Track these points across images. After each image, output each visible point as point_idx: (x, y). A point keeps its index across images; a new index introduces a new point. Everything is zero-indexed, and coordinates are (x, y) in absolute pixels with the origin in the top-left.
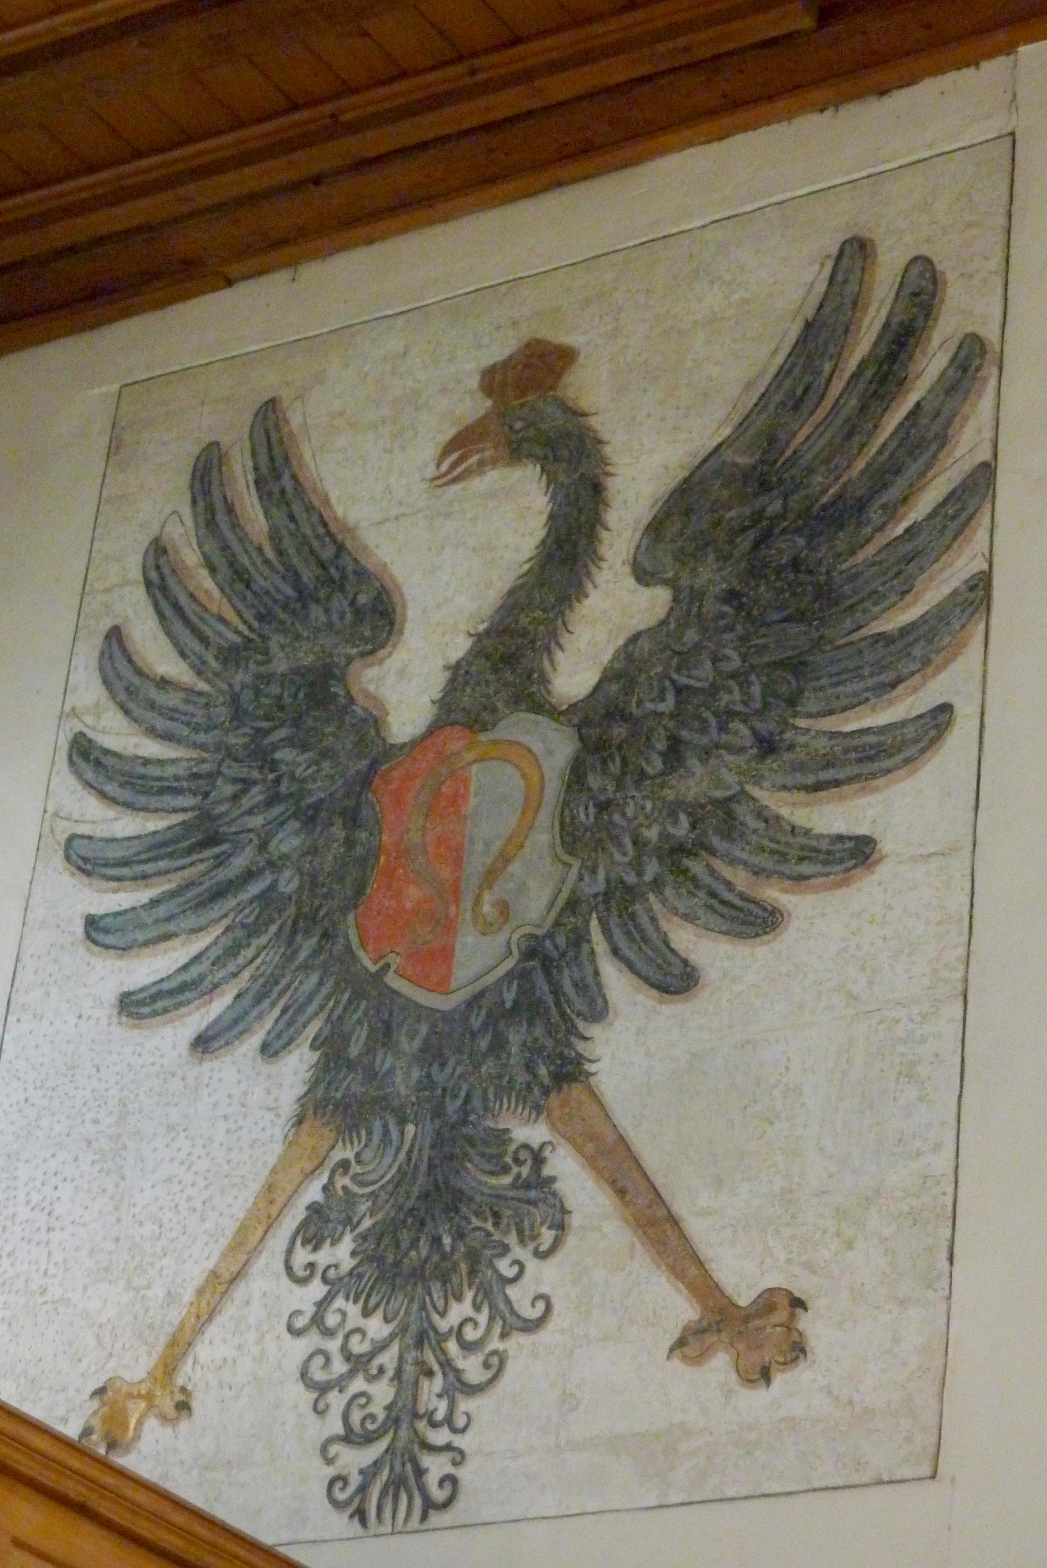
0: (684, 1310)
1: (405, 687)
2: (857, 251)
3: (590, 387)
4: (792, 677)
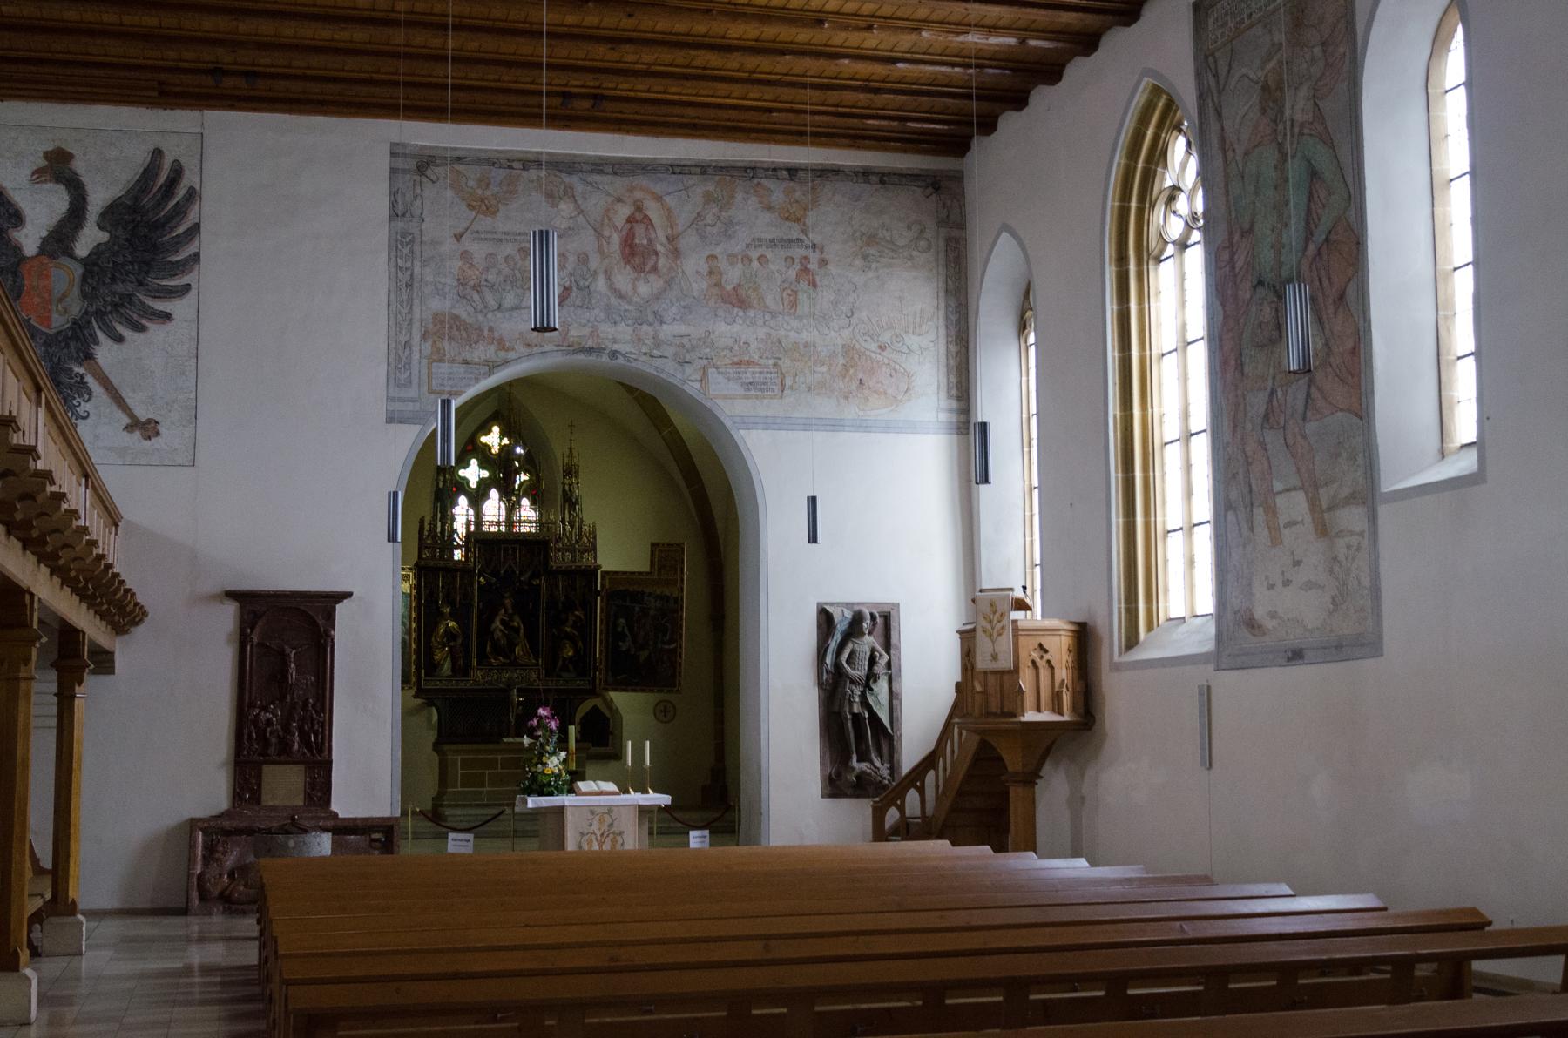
0: (126, 420)
1: (29, 239)
2: (157, 153)
3: (79, 166)
4: (147, 267)
